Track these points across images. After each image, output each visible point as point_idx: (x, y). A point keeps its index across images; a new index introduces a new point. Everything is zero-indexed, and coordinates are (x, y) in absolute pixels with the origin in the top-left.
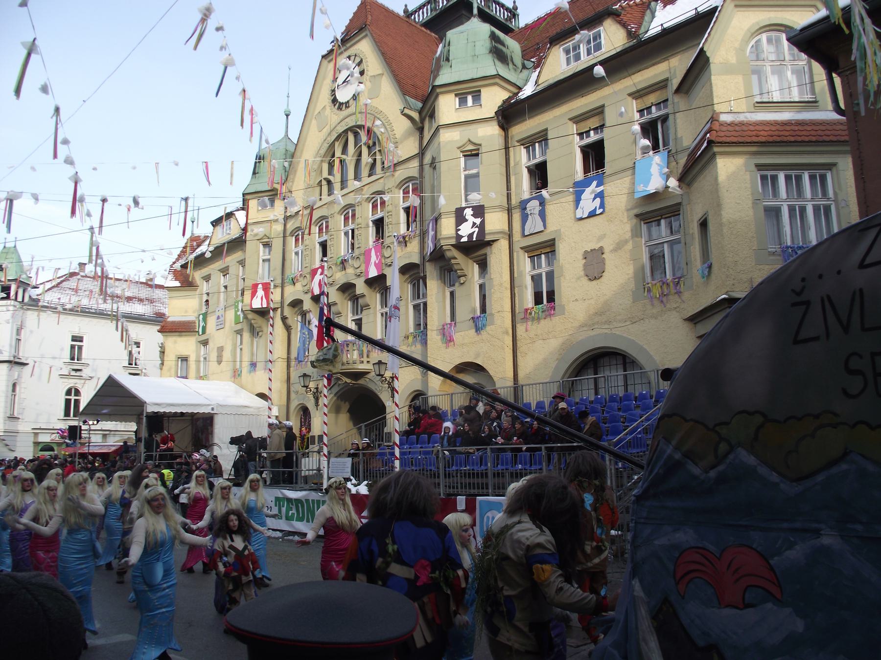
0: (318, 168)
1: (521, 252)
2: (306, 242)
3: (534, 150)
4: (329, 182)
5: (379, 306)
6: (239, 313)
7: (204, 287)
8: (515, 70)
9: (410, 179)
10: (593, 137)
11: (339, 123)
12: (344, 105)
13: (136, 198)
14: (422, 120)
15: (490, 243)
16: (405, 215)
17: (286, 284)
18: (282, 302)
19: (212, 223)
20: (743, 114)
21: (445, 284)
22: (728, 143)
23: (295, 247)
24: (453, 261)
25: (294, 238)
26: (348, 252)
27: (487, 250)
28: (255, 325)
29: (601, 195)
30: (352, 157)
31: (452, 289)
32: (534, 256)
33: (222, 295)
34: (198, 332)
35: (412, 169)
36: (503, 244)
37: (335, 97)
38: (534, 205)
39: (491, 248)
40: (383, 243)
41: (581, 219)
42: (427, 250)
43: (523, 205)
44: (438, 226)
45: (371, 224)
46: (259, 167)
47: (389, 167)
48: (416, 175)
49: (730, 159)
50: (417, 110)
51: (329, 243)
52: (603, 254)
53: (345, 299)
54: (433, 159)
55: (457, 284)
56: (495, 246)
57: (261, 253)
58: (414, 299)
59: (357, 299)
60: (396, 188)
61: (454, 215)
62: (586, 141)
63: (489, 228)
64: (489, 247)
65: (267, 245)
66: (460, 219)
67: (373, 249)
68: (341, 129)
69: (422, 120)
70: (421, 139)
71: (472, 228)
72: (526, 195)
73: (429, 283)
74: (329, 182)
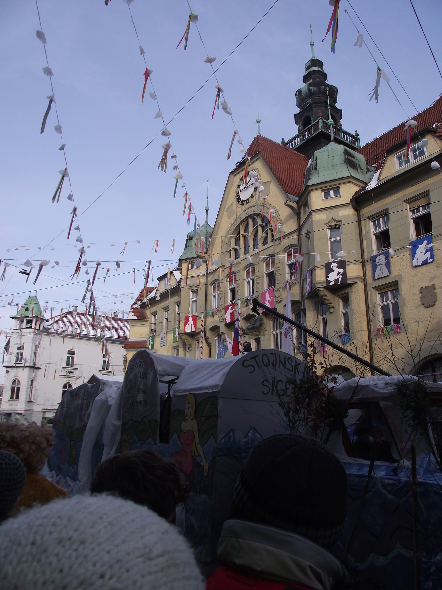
0: (229, 242)
1: (373, 290)
2: (221, 289)
3: (379, 223)
4: (236, 250)
5: (272, 330)
6: (177, 335)
7: (153, 319)
8: (362, 172)
10: (422, 211)
12: (245, 202)
14: (299, 208)
15: (350, 285)
16: (289, 269)
17: (208, 316)
18: (205, 328)
19: (158, 279)
24: (324, 298)
25: (213, 287)
27: (349, 290)
28: (187, 343)
29: (431, 250)
31: (324, 317)
32: (383, 293)
33: (164, 324)
34: (149, 348)
35: (294, 239)
36: (360, 285)
37: (239, 196)
38: (381, 259)
39: (351, 288)
40: (274, 288)
41: (417, 266)
42: (305, 291)
43: (373, 259)
44: (313, 276)
45: (265, 275)
46: (189, 243)
47: (277, 240)
48: (296, 243)
50: (295, 202)
51: (237, 289)
52: (434, 289)
54: (308, 233)
55: (328, 313)
56: (354, 287)
57: (191, 297)
60: (282, 252)
61: (324, 267)
62: (417, 215)
63: (349, 275)
64: (350, 288)
65: (195, 292)
66: (329, 269)
68: (243, 217)
69: (299, 208)
71: (337, 276)
72: (375, 253)
73: (307, 313)
74: (236, 250)
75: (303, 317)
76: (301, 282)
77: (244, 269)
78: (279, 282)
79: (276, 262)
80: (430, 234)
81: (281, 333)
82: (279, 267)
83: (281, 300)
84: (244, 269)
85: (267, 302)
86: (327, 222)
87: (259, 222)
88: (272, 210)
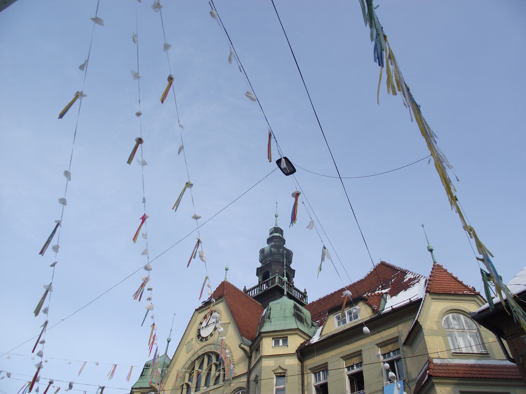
3: (319, 375)
4: (188, 386)
9: (240, 388)
10: (356, 369)
11: (200, 349)
12: (204, 339)
13: (72, 383)
14: (251, 352)
20: (446, 360)
22: (441, 377)
30: (206, 370)
37: (200, 333)
46: (145, 371)
47: (227, 380)
48: (244, 385)
49: (444, 387)
50: (249, 345)
54: (257, 377)
62: (352, 372)
68: (200, 353)
69: (251, 352)
70: (250, 363)
74: (188, 386)
80: (362, 391)
86: (274, 369)
87: (214, 360)
88: (227, 351)
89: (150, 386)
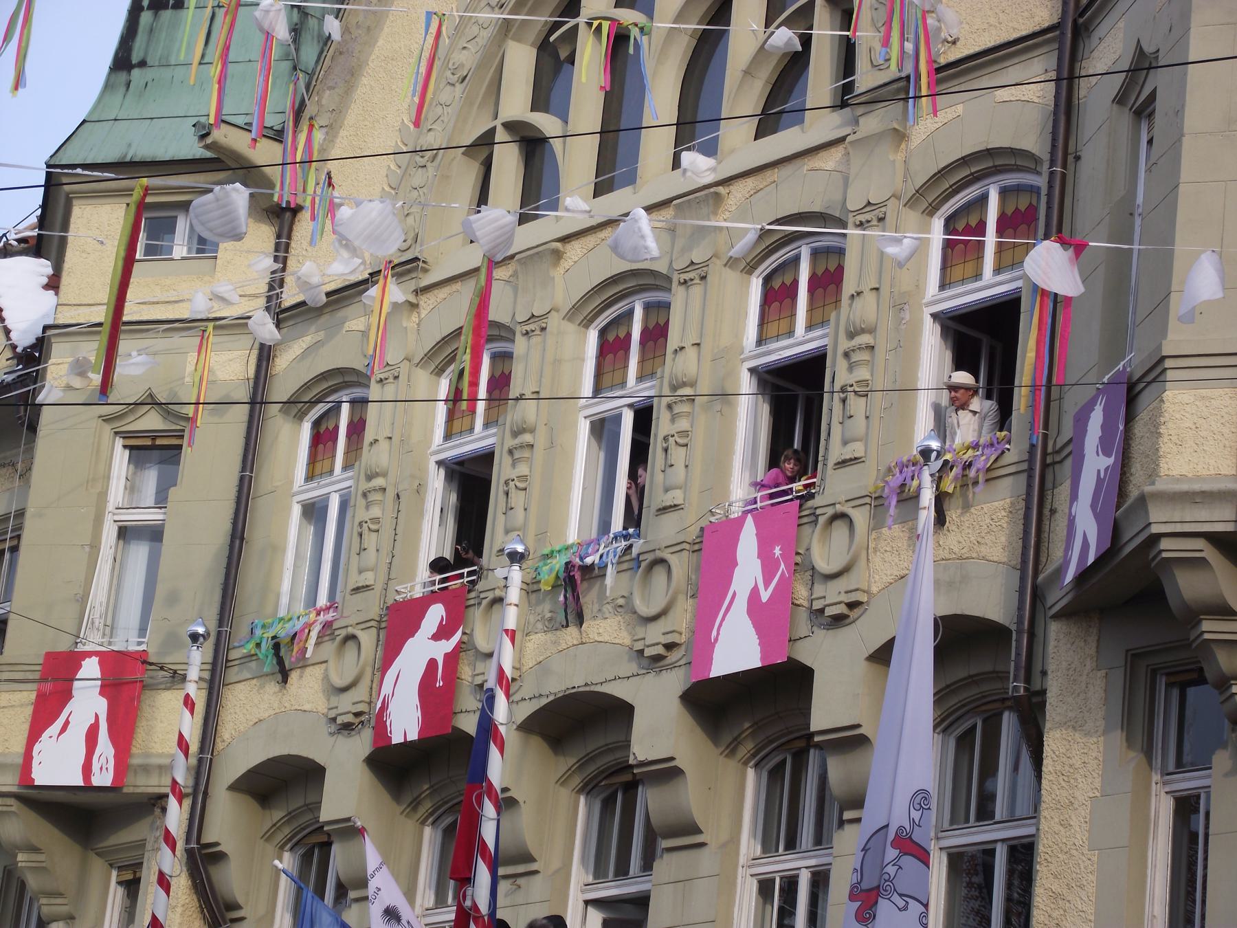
0: (482, 65)
2: (376, 455)
17: (233, 674)
18: (203, 771)
21: (1148, 752)
23: (310, 477)
24: (1211, 628)
26: (605, 526)
28: (33, 882)
30: (679, 18)
31: (1188, 782)
42: (1057, 553)
44: (1139, 429)
47: (876, 97)
48: (1033, 140)
51: (502, 471)
53: (563, 781)
57: (117, 493)
58: (958, 818)
59: (631, 787)
60: (911, 203)
67: (749, 524)
73: (1053, 742)
75: (1016, 768)
76: (1030, 471)
77: (582, 314)
78: (856, 449)
79: (849, 286)
81: (820, 880)
82: (871, 331)
83: (852, 605)
84: (582, 314)
85: (741, 605)
89: (207, 147)
